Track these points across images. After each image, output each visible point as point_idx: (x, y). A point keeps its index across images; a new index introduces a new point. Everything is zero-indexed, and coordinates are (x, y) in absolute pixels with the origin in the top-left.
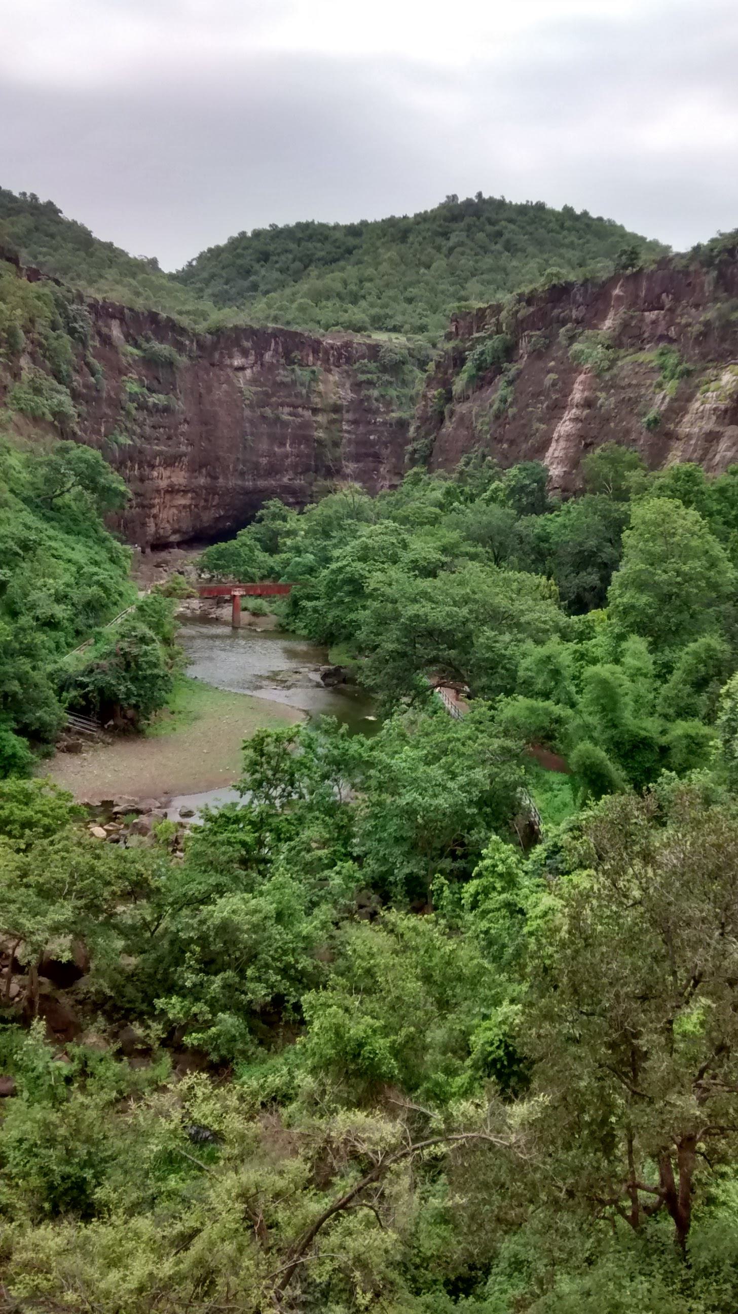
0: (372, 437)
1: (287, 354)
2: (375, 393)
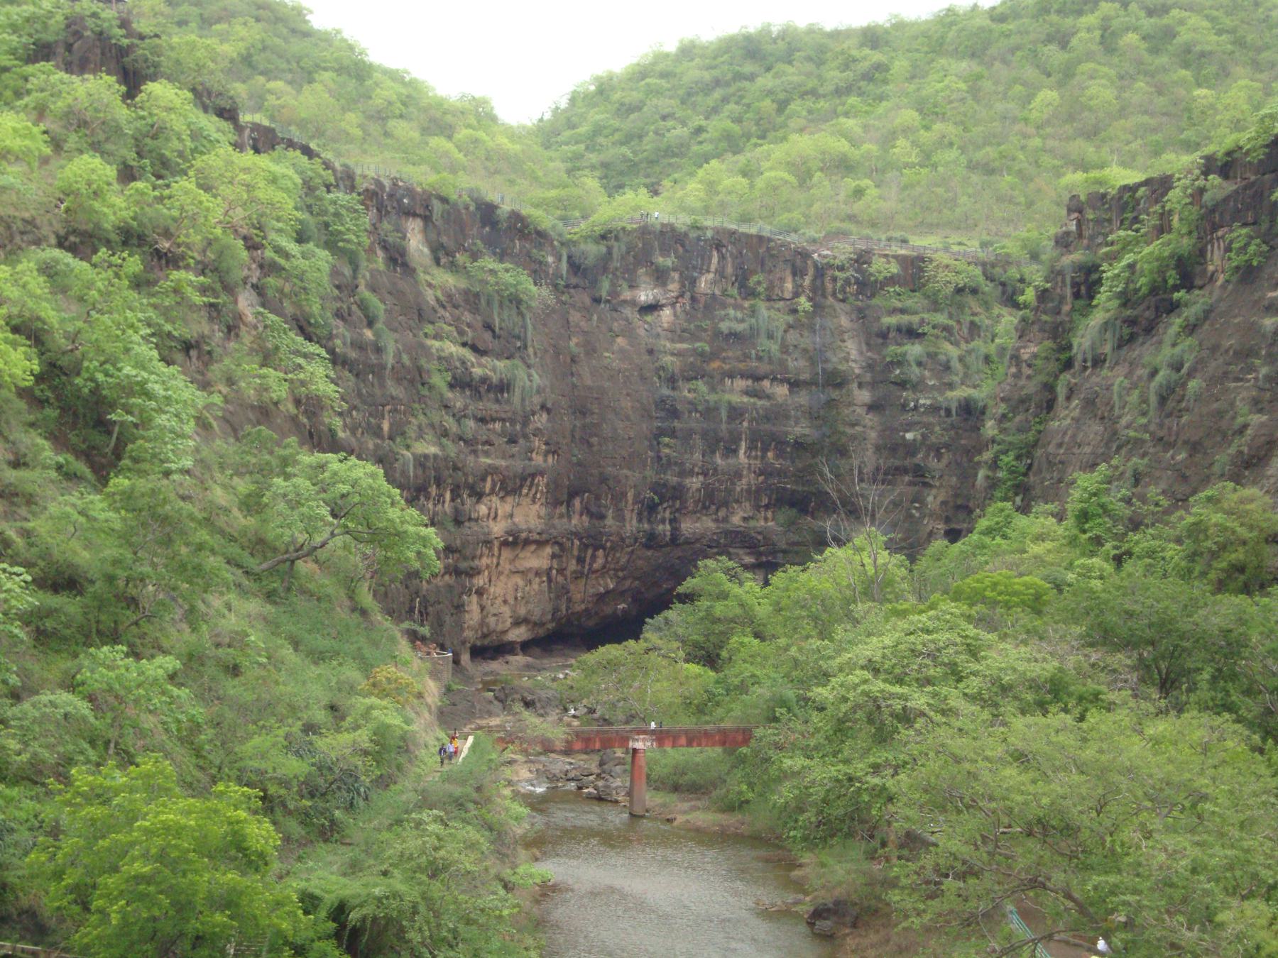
0: (909, 436)
1: (742, 280)
2: (914, 350)
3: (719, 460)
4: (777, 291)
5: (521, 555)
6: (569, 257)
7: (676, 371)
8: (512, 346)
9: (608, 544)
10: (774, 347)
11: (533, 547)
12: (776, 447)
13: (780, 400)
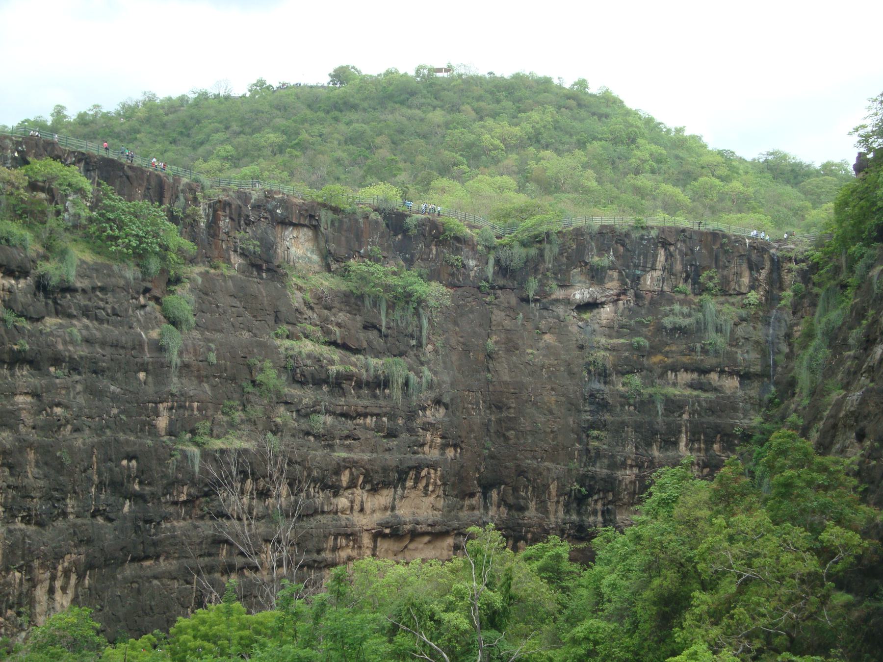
1: (693, 276)
3: (656, 452)
4: (733, 285)
5: (411, 546)
6: (498, 261)
7: (609, 365)
8: (402, 343)
9: (529, 536)
10: (720, 341)
11: (426, 539)
12: (722, 440)
13: (728, 392)
